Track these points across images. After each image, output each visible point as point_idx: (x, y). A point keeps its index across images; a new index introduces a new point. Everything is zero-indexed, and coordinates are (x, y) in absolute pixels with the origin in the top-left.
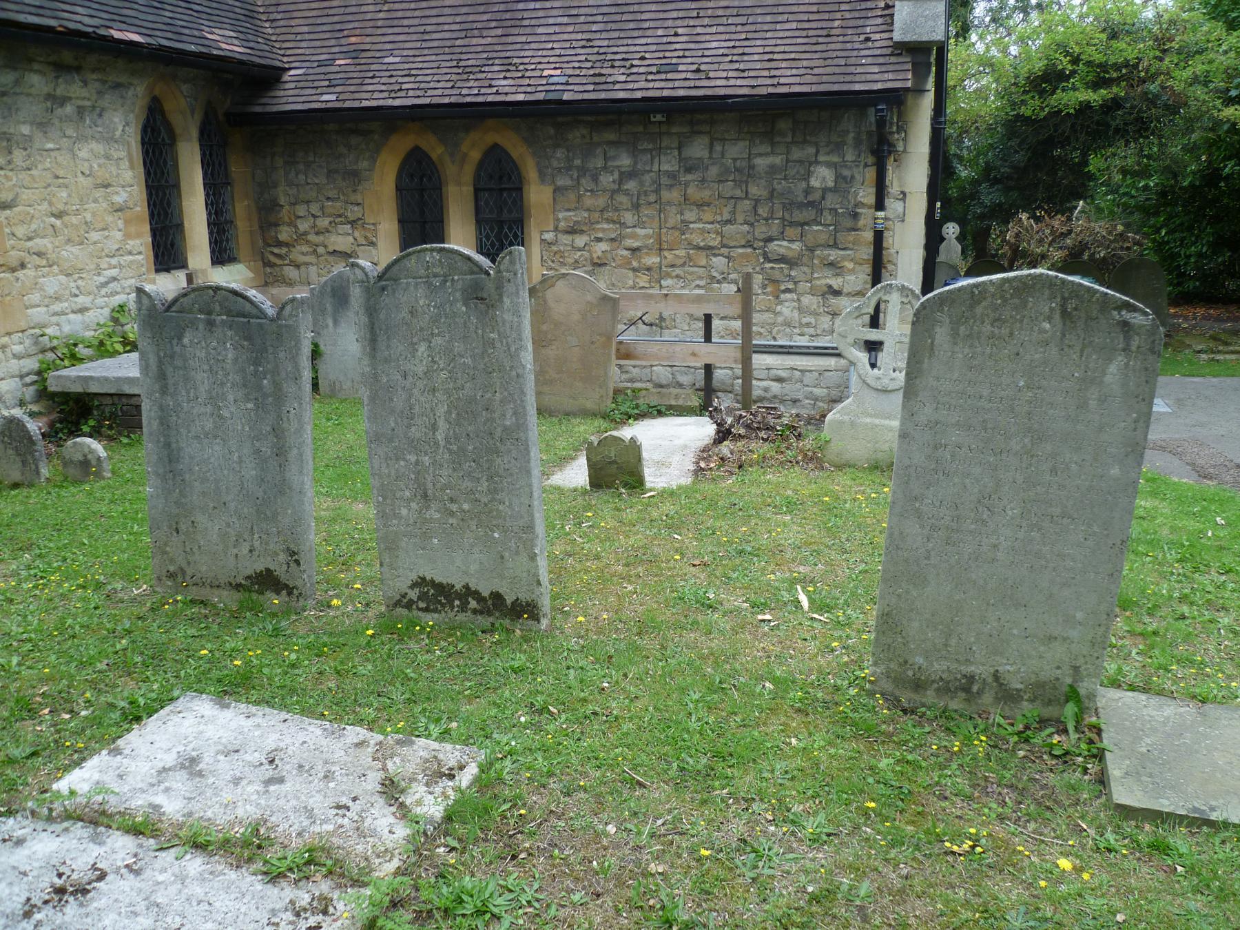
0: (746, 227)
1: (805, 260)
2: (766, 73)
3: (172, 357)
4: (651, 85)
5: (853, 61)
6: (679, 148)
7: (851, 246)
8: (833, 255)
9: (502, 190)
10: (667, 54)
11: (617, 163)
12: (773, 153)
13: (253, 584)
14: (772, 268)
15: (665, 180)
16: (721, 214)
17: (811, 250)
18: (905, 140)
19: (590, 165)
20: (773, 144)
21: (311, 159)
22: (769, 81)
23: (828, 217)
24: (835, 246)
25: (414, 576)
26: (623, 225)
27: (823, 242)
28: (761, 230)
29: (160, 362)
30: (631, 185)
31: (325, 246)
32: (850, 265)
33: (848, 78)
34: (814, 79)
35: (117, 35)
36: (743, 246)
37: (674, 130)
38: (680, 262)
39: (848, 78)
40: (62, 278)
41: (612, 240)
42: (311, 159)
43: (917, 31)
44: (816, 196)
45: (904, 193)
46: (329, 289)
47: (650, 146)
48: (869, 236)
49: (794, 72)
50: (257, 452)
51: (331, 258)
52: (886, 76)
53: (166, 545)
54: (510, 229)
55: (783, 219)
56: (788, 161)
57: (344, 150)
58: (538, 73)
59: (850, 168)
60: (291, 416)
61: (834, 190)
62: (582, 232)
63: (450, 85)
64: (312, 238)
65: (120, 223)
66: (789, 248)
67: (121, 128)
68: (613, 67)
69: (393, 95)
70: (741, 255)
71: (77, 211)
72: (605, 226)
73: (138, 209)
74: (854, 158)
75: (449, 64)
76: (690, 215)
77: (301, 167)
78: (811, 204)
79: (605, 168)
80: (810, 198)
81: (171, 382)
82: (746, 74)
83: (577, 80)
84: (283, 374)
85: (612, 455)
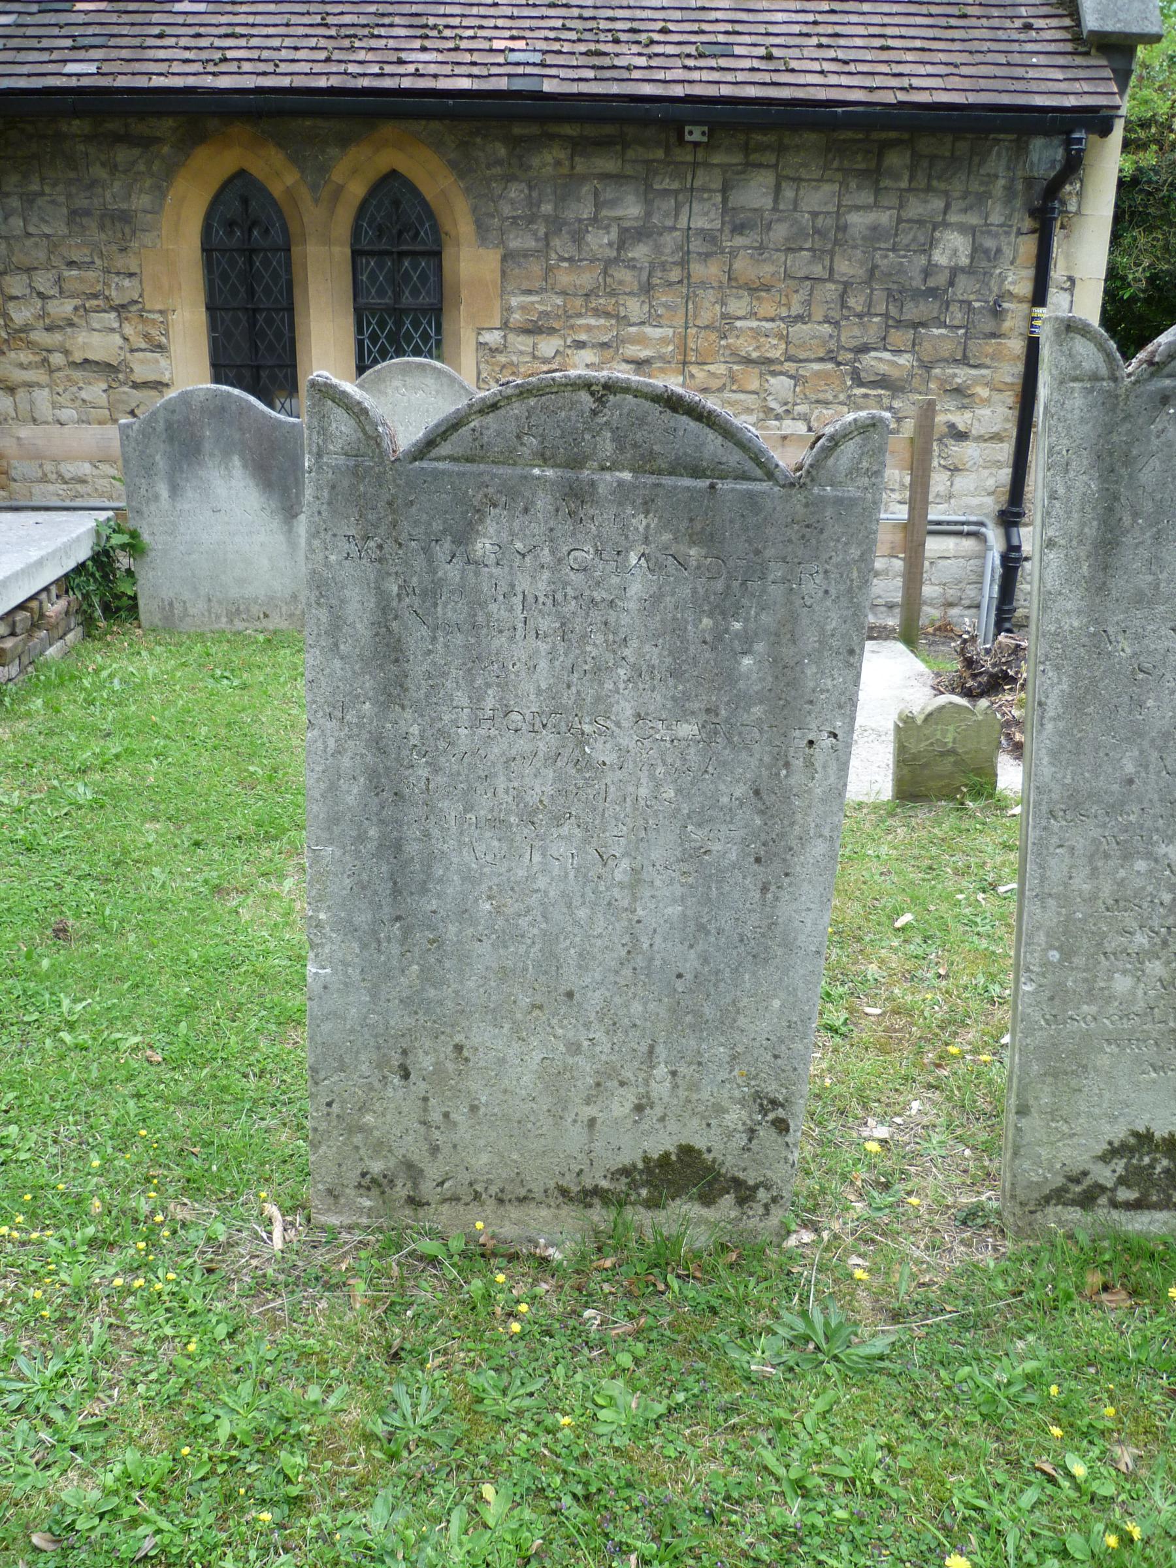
0: (827, 329)
1: (915, 382)
2: (884, 68)
3: (431, 593)
4: (695, 75)
5: (1017, 59)
6: (725, 190)
7: (988, 361)
8: (962, 375)
9: (402, 254)
10: (706, 27)
11: (619, 213)
12: (876, 205)
13: (634, 1185)
14: (866, 396)
15: (696, 245)
16: (788, 306)
17: (927, 367)
18: (1080, 194)
19: (570, 215)
20: (877, 191)
21: (35, 187)
22: (894, 82)
23: (956, 315)
24: (965, 361)
25: (1118, 1132)
26: (623, 320)
27: (947, 355)
28: (851, 334)
29: (385, 611)
30: (640, 252)
31: (66, 353)
32: (983, 392)
33: (1019, 86)
34: (967, 84)
36: (821, 360)
37: (716, 159)
38: (715, 384)
39: (1019, 86)
41: (604, 345)
42: (35, 187)
43: (1122, 16)
44: (941, 280)
45: (1071, 279)
46: (161, 426)
47: (675, 185)
48: (1017, 346)
49: (930, 69)
50: (694, 855)
51: (77, 375)
52: (1077, 86)
53: (363, 1109)
54: (416, 324)
55: (886, 316)
56: (899, 220)
57: (101, 173)
58: (485, 45)
59: (996, 236)
60: (819, 757)
61: (970, 271)
62: (552, 331)
63: (323, 55)
64: (39, 336)
66: (894, 363)
68: (616, 41)
69: (211, 68)
70: (817, 374)
72: (592, 321)
74: (1002, 219)
75: (306, 20)
76: (737, 306)
77: (15, 202)
78: (932, 292)
79: (595, 220)
80: (931, 283)
81: (418, 669)
82: (852, 68)
83: (561, 60)
84: (810, 639)
85: (949, 739)
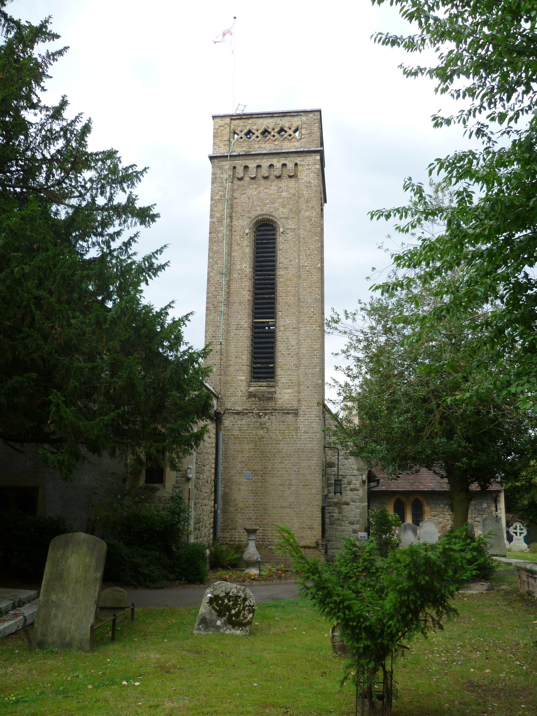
23: (486, 513)
78: (483, 511)
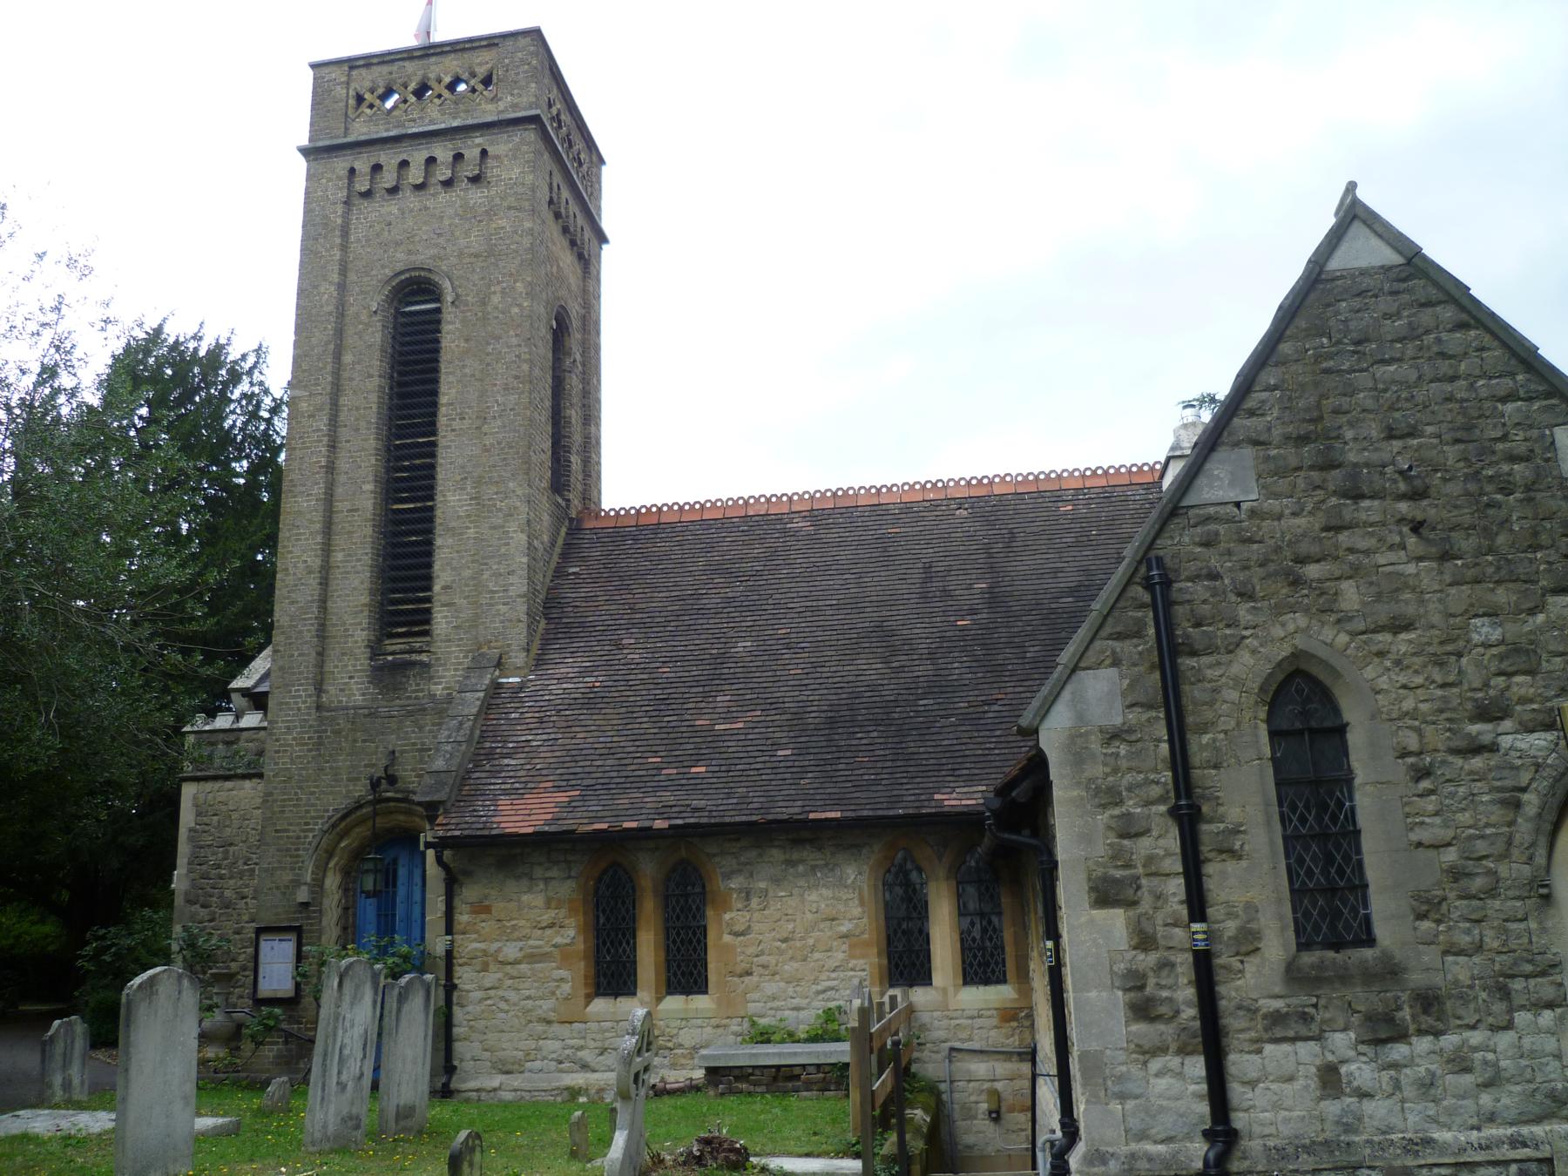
35: (812, 816)
40: (782, 984)
65: (845, 947)
67: (853, 877)
71: (802, 938)
73: (866, 936)
